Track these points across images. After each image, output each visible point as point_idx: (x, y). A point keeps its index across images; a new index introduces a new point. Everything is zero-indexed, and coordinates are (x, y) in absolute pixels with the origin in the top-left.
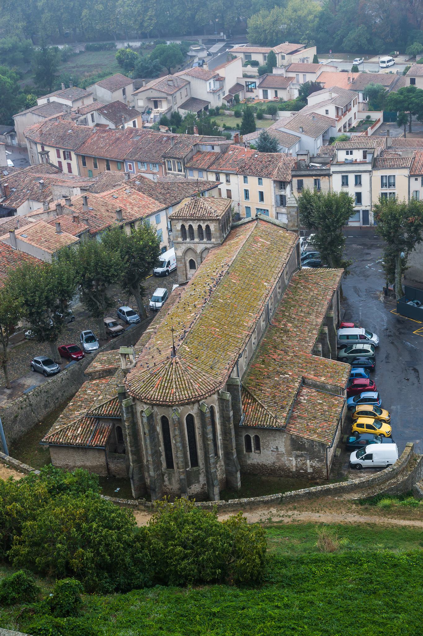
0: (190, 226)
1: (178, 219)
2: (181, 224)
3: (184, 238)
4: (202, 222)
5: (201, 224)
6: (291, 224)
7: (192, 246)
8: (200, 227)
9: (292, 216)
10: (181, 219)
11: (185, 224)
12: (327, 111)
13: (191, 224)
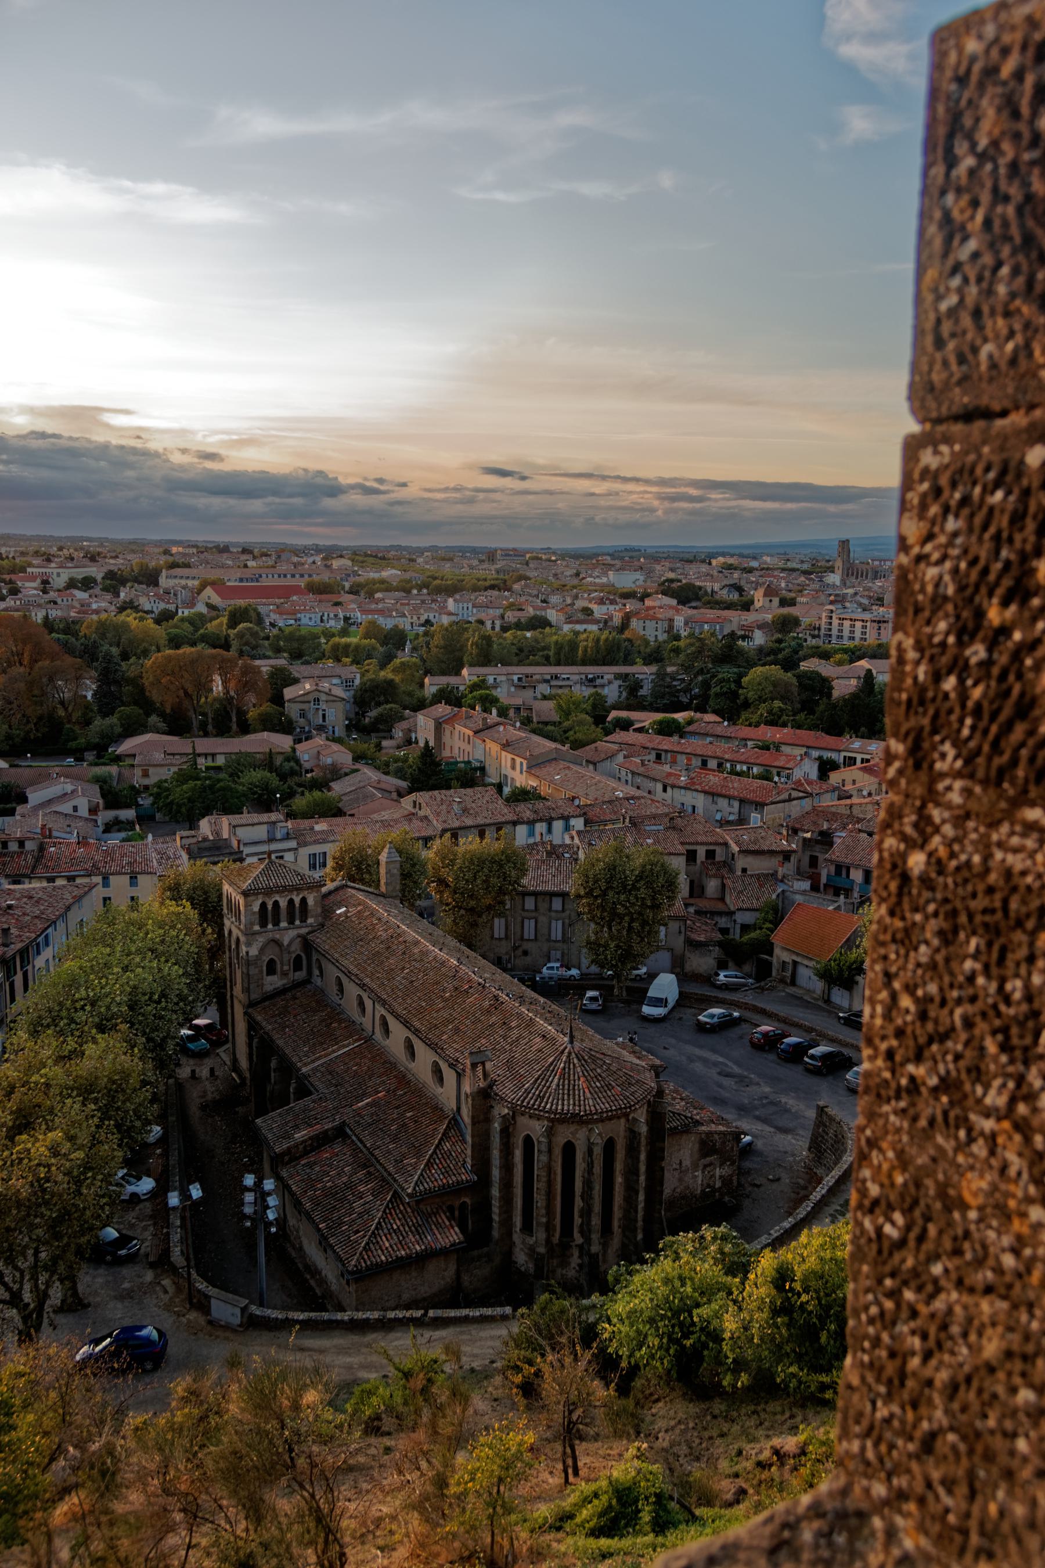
0: (276, 903)
3: (263, 924)
8: (291, 902)
9: (392, 875)
11: (267, 900)
12: (75, 809)
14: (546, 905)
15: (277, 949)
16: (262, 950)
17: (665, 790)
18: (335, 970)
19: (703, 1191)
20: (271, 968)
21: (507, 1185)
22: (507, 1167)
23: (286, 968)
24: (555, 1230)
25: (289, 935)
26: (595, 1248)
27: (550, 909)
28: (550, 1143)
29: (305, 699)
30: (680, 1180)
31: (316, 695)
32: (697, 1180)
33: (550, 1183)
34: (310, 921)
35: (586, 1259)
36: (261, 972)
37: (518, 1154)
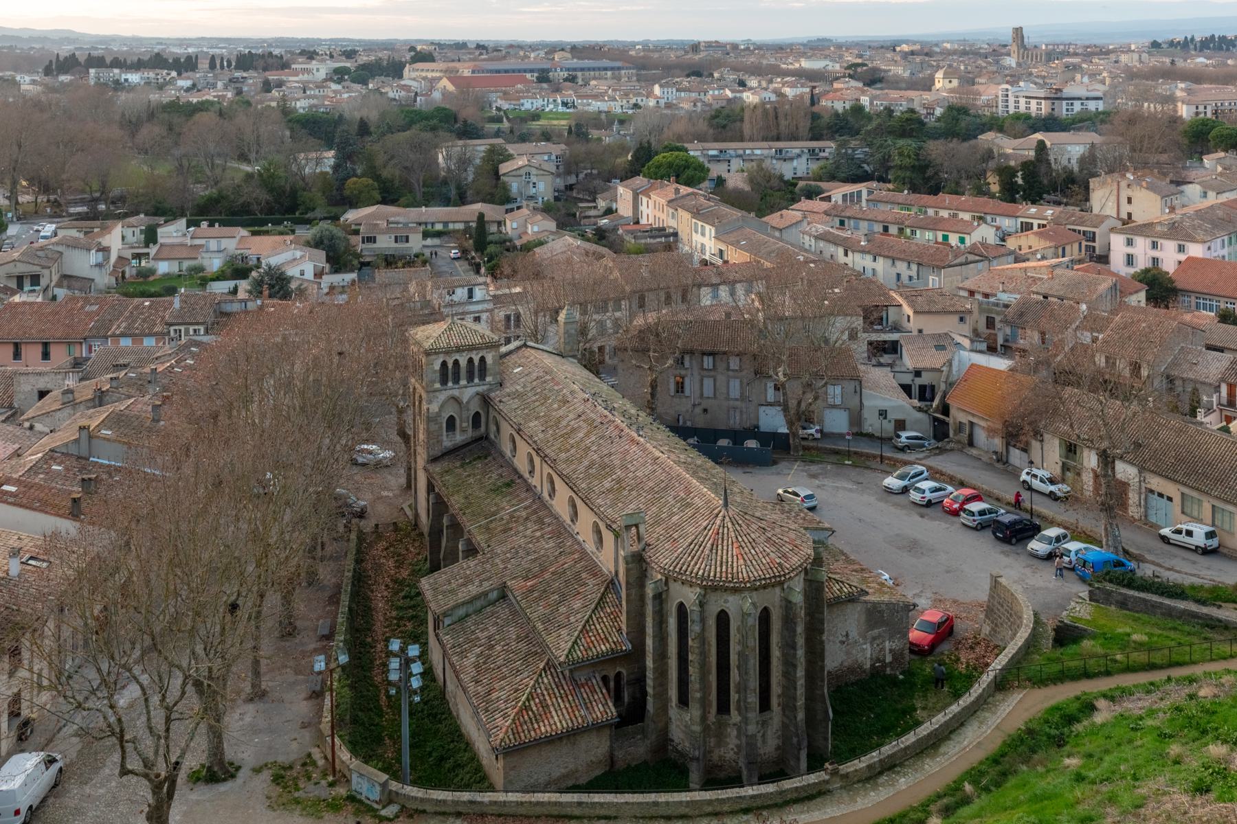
0: (456, 363)
1: (436, 353)
2: (441, 360)
3: (444, 382)
4: (475, 352)
5: (473, 356)
6: (568, 348)
7: (456, 393)
8: (471, 361)
10: (441, 353)
13: (458, 358)
14: (724, 365)
15: (456, 406)
16: (442, 406)
17: (846, 255)
18: (509, 427)
19: (872, 666)
20: (451, 423)
21: (661, 656)
22: (661, 638)
23: (464, 425)
24: (710, 705)
25: (468, 392)
26: (752, 729)
27: (728, 369)
28: (702, 612)
29: (518, 173)
30: (848, 653)
31: (527, 169)
32: (865, 654)
33: (704, 655)
34: (489, 379)
35: (744, 739)
36: (441, 427)
37: (672, 623)
